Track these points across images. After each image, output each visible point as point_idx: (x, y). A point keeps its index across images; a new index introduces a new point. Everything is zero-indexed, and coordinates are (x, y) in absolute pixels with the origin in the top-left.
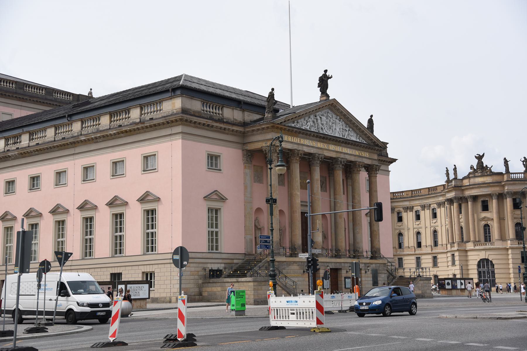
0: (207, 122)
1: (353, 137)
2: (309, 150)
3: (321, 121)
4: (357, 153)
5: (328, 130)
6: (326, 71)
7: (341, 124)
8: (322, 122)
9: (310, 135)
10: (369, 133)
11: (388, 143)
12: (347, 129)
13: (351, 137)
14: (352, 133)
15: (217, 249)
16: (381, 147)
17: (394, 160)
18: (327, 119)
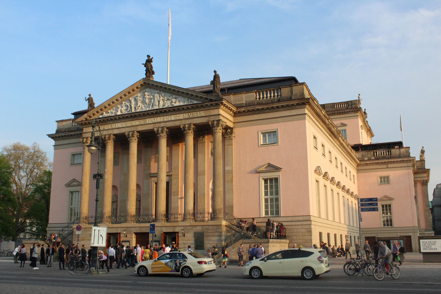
0: (65, 134)
2: (118, 132)
12: (170, 99)
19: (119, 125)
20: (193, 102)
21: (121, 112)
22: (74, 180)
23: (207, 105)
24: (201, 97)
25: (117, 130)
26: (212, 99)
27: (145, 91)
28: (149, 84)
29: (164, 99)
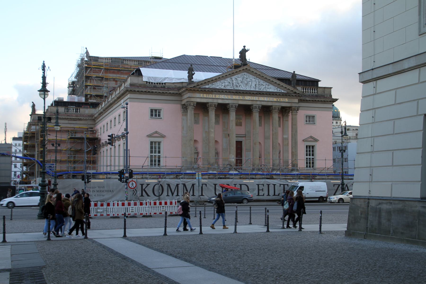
1: (272, 89)
3: (237, 81)
4: (275, 99)
5: (244, 86)
6: (244, 47)
7: (257, 81)
8: (238, 82)
9: (222, 92)
10: (285, 85)
11: (331, 88)
12: (264, 84)
13: (267, 89)
14: (271, 86)
15: (159, 165)
16: (298, 94)
17: (336, 100)
18: (243, 79)
19: (222, 96)
20: (281, 91)
21: (224, 86)
22: (156, 132)
23: (293, 96)
24: (289, 89)
25: (221, 100)
26: (297, 92)
27: (243, 74)
28: (249, 70)
29: (259, 84)
